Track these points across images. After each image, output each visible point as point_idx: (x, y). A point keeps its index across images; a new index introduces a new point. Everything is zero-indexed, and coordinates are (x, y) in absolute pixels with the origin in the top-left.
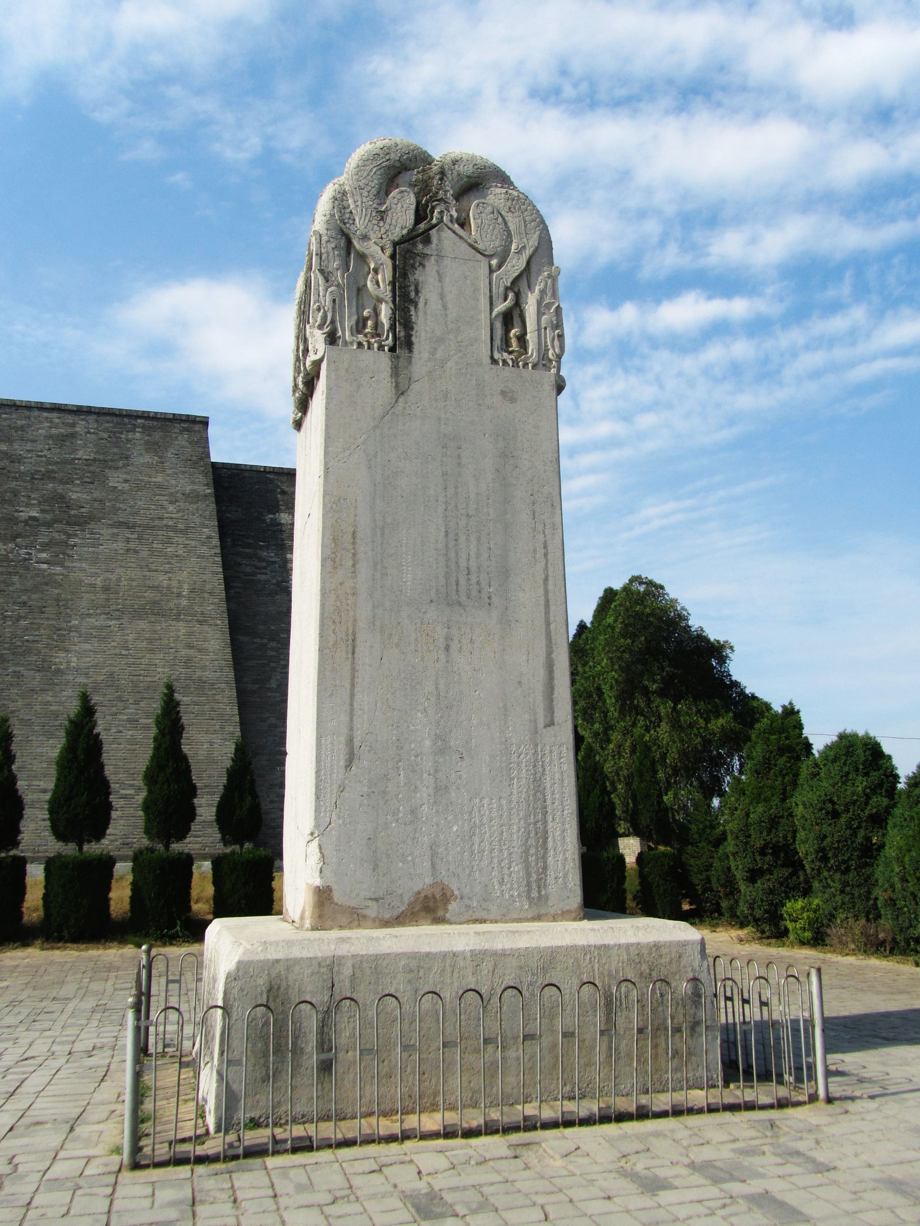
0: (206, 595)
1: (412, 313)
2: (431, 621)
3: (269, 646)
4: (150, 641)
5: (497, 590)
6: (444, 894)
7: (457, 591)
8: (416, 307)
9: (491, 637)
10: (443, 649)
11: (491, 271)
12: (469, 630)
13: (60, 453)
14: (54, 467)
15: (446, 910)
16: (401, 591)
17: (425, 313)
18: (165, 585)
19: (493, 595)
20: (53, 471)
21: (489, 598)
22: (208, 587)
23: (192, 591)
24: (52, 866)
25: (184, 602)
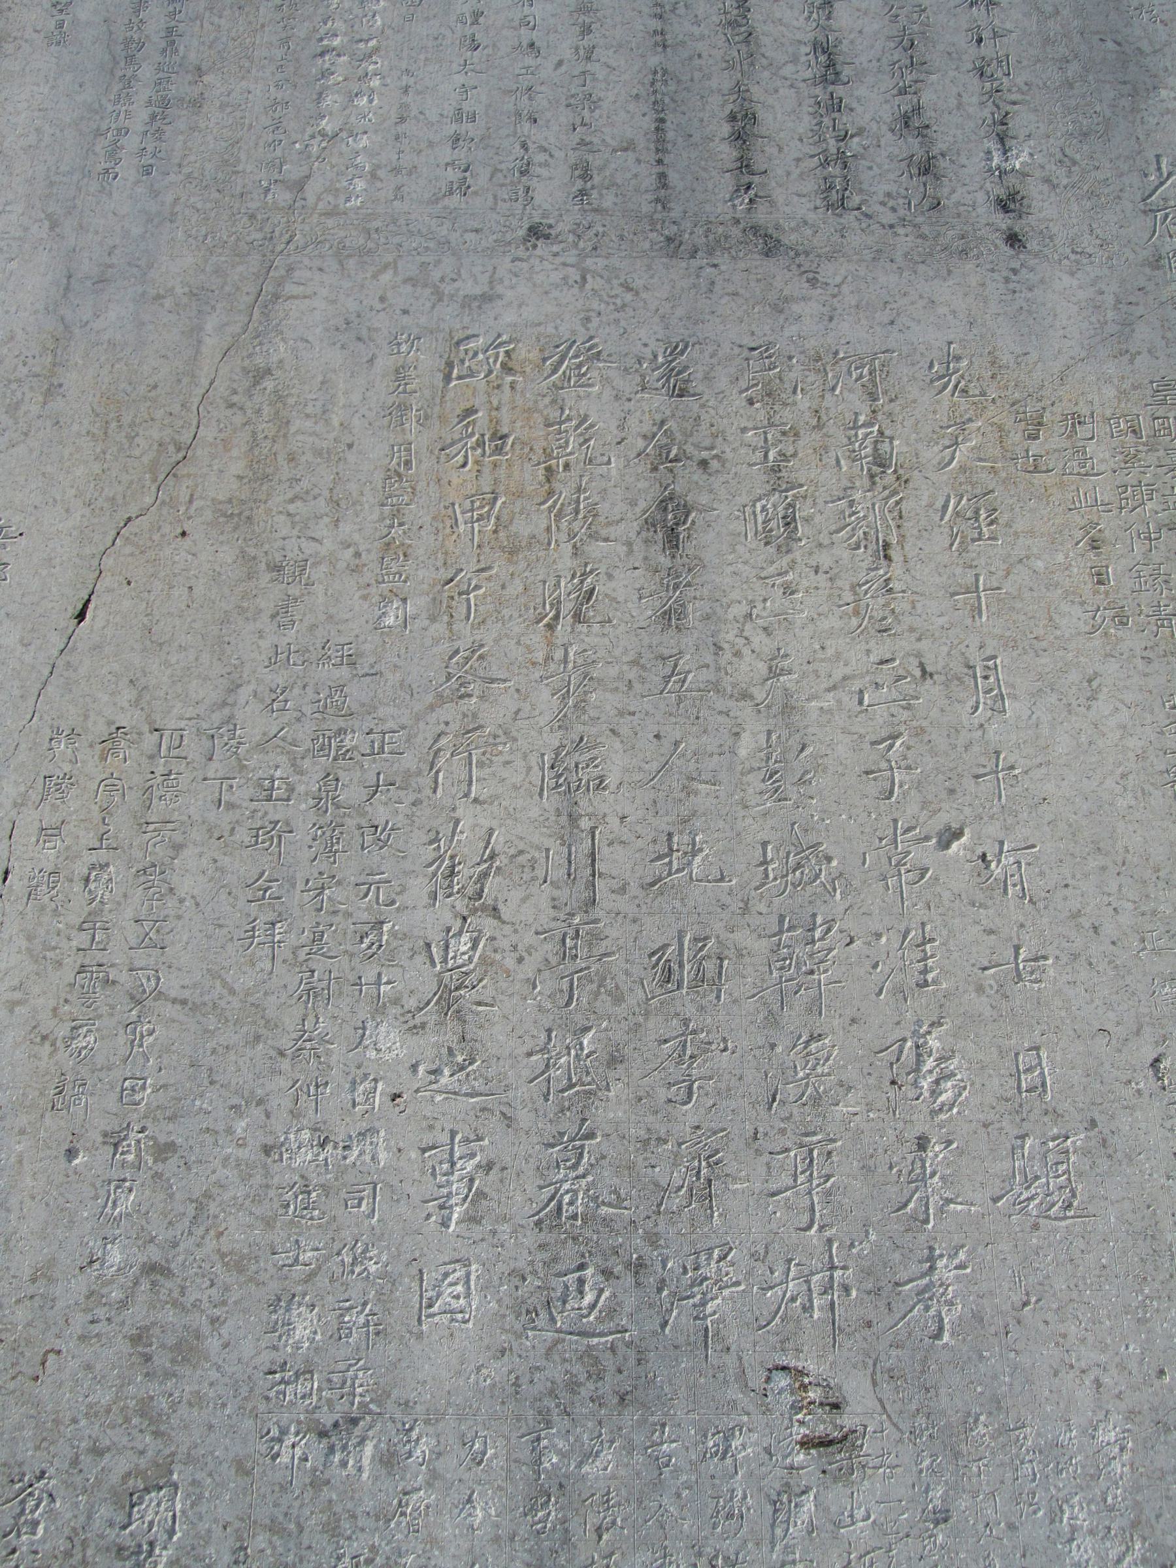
2: (526, 352)
5: (1066, 160)
7: (744, 165)
9: (1051, 440)
10: (630, 528)
12: (857, 403)
16: (299, 186)
19: (1034, 190)
21: (1008, 204)
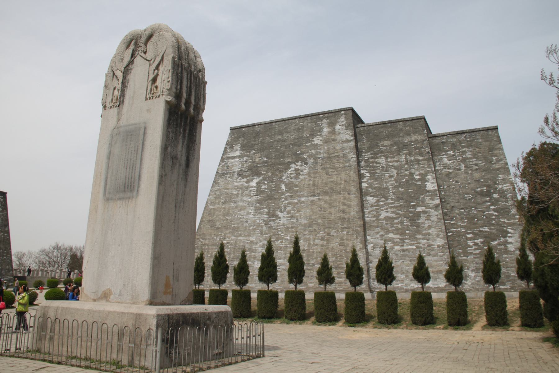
0: (351, 182)
1: (126, 91)
3: (380, 200)
4: (330, 204)
6: (110, 292)
8: (127, 88)
11: (150, 65)
13: (298, 135)
14: (296, 141)
15: (110, 298)
17: (129, 89)
18: (335, 180)
20: (296, 142)
22: (352, 179)
23: (345, 181)
24: (234, 292)
25: (342, 186)
